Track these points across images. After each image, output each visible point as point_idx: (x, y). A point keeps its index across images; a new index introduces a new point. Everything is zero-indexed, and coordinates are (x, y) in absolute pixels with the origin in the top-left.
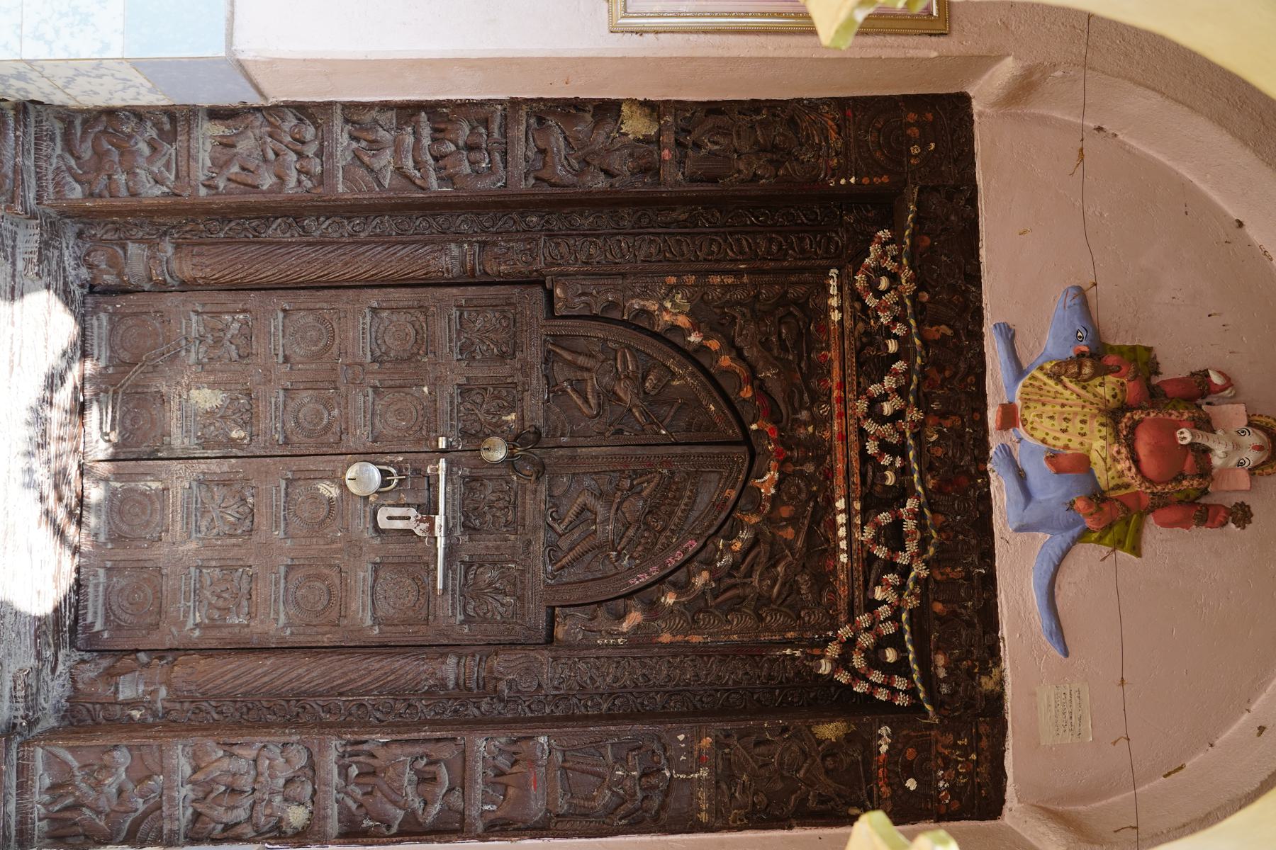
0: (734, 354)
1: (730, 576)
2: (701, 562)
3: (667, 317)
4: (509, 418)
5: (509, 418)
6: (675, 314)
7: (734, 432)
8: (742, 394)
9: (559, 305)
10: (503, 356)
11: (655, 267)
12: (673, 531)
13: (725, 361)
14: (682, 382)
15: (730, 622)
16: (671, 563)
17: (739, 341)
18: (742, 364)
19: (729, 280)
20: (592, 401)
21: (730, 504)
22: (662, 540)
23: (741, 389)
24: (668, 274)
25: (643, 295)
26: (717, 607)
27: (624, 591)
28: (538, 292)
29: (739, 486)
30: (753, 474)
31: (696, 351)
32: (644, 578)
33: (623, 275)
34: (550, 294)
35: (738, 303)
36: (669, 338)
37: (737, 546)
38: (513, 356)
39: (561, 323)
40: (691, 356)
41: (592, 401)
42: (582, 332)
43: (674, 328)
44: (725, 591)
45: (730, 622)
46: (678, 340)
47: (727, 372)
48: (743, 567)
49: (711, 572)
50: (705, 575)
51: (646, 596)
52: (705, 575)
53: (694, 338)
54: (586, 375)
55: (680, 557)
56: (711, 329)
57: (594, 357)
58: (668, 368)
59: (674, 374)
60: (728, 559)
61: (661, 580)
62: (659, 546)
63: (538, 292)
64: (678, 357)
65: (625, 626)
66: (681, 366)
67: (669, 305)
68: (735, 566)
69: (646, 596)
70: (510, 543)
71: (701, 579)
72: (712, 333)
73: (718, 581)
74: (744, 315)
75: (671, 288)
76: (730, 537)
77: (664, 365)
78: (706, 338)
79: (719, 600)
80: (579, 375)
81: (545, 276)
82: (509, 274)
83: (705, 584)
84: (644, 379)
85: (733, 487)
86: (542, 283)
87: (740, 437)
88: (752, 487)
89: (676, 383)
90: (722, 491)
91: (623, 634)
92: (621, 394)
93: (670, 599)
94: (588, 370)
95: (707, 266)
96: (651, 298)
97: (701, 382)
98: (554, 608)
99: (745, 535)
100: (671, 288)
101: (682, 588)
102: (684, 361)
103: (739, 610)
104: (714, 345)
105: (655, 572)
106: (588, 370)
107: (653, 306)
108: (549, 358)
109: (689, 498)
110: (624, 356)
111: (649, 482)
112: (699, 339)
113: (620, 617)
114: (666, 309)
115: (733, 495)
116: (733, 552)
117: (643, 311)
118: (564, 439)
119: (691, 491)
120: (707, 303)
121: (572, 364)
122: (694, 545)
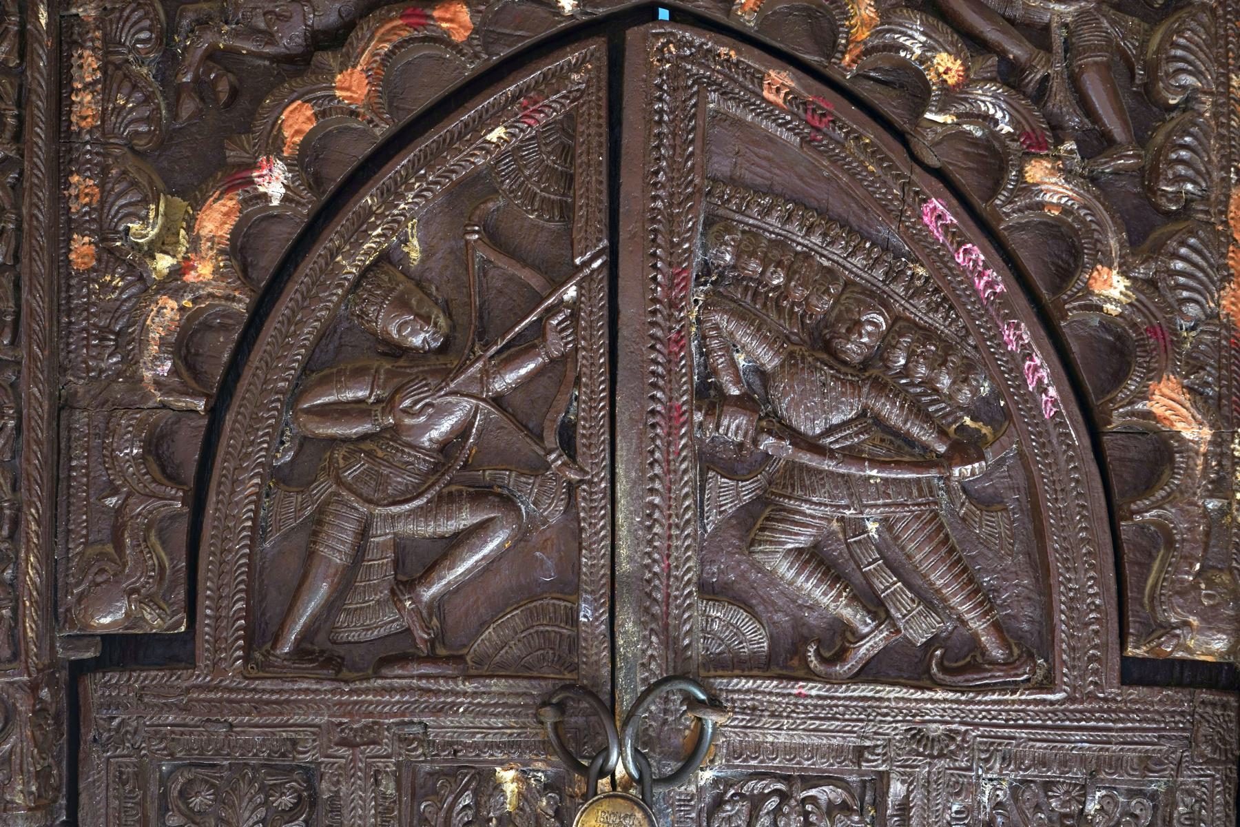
0: (327, 58)
1: (1042, 92)
2: (994, 193)
3: (204, 270)
4: (510, 788)
5: (510, 788)
6: (195, 242)
7: (580, 67)
8: (459, 36)
9: (153, 621)
10: (308, 801)
11: (36, 301)
12: (893, 275)
13: (352, 85)
14: (411, 228)
15: (1188, 104)
16: (992, 281)
17: (291, 38)
18: (363, 31)
19: (88, 64)
20: (465, 519)
21: (813, 92)
22: (918, 310)
23: (443, 40)
24: (60, 262)
25: (128, 342)
26: (1141, 140)
27: (1077, 436)
28: (97, 688)
29: (752, 59)
30: (719, 16)
31: (316, 183)
32: (1040, 370)
33: (62, 406)
34: (123, 650)
35: (165, 38)
36: (271, 265)
37: (948, 65)
38: (310, 775)
39: (206, 611)
40: (334, 194)
41: (465, 519)
42: (240, 547)
43: (240, 249)
44: (1087, 109)
45: (1191, 98)
46: (282, 237)
47: (388, 82)
48: (1016, 50)
49: (1028, 156)
50: (1037, 171)
51: (1100, 367)
52: (1037, 171)
53: (274, 184)
54: (381, 536)
55: (973, 254)
56: (248, 130)
57: (321, 510)
58: (365, 272)
59: (385, 258)
60: (988, 100)
61: (1048, 321)
62: (937, 320)
63: (97, 688)
64: (332, 238)
65: (1194, 432)
66: (360, 230)
67: (164, 263)
68: (1010, 76)
69: (1100, 367)
70: (917, 798)
71: (1050, 184)
72: (260, 126)
73: (1058, 132)
74: (203, 23)
75: (109, 256)
76: (914, 87)
77: (356, 284)
78: (274, 146)
79: (1118, 132)
80: (380, 563)
81: (54, 664)
82: (42, 776)
83: (1068, 174)
84: (397, 351)
85: (759, 78)
86: (79, 669)
87: (595, 47)
88: (763, 21)
89: (414, 251)
90: (770, 111)
91: (1220, 442)
92: (446, 425)
93: (1112, 287)
94: (364, 532)
95: (40, 133)
96: (137, 317)
97: (413, 167)
98: (1125, 660)
99: (913, 40)
100: (111, 254)
101: (1075, 252)
102: (344, 221)
103: (1152, 69)
104: (297, 121)
105: (1019, 334)
106: (364, 532)
107: (166, 313)
108: (324, 656)
109: (788, 219)
110: (324, 412)
111: (730, 347)
112: (279, 168)
113: (1161, 450)
114: (177, 272)
115: (779, 82)
116: (967, 82)
117: (186, 345)
118: (586, 614)
119: (767, 211)
120: (165, 140)
121: (346, 583)
122: (938, 211)
